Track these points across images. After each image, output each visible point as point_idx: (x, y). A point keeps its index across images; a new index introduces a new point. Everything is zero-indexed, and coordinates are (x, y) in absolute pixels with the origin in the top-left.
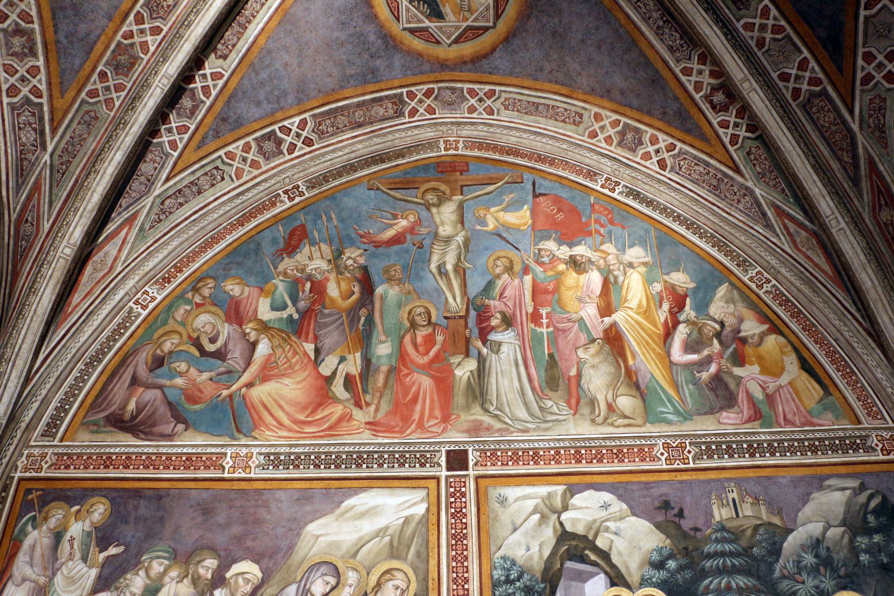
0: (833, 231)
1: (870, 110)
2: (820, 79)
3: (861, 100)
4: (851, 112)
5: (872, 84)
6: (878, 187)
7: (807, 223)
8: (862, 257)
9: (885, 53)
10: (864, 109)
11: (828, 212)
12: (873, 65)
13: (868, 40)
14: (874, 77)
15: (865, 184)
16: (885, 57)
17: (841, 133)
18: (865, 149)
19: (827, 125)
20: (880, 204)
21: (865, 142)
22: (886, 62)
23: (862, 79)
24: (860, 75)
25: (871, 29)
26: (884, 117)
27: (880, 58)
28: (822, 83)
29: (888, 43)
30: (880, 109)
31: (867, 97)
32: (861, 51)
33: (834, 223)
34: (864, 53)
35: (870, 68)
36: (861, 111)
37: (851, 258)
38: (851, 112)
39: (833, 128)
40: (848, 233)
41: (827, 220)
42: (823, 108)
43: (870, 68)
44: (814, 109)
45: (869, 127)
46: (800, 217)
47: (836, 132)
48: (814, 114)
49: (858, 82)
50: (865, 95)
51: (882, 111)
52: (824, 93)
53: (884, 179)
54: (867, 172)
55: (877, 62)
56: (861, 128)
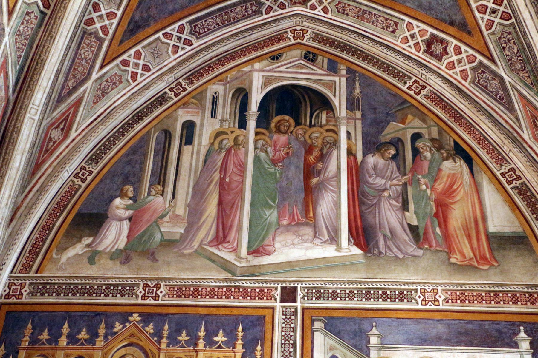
0: (28, 115)
1: (110, 78)
2: (108, 32)
3: (112, 68)
4: (102, 67)
5: (125, 68)
6: (68, 116)
7: (11, 90)
8: (28, 146)
9: (145, 63)
10: (108, 74)
11: (37, 103)
12: (135, 61)
13: (147, 48)
14: (129, 66)
15: (63, 107)
16: (144, 65)
17: (84, 69)
18: (85, 91)
19: (83, 56)
20: (59, 125)
21: (89, 88)
22: (141, 67)
23: (124, 60)
24: (125, 57)
25: (154, 45)
26: (112, 90)
27: (141, 62)
28: (107, 35)
29: (151, 60)
30: (114, 83)
31: (115, 71)
32: (139, 47)
33: (33, 111)
34: (139, 50)
35: (132, 61)
36: (106, 73)
37: (21, 140)
38: (102, 67)
39: (84, 62)
40: (35, 125)
41: (31, 105)
42: (91, 47)
43: (132, 61)
44: (87, 41)
45: (100, 85)
46: (11, 83)
47: (82, 65)
48: (85, 43)
49: (121, 59)
50: (116, 68)
51: (114, 86)
52: (101, 41)
53: (76, 117)
54: (72, 103)
55: (138, 61)
56: (96, 81)
